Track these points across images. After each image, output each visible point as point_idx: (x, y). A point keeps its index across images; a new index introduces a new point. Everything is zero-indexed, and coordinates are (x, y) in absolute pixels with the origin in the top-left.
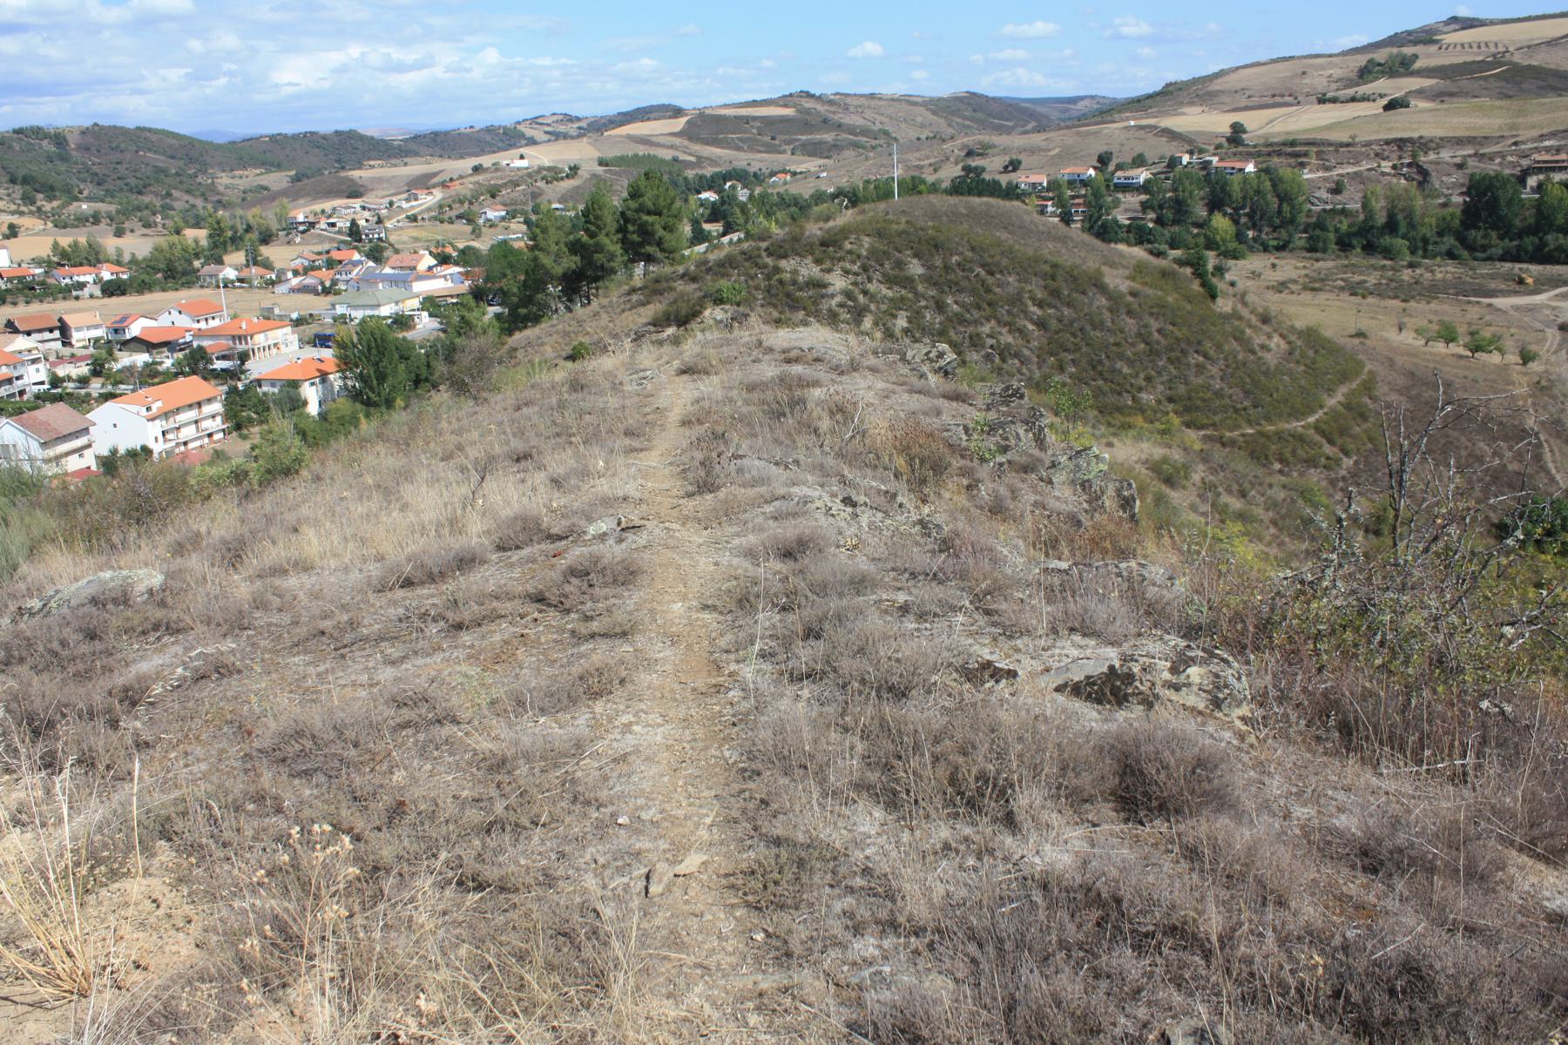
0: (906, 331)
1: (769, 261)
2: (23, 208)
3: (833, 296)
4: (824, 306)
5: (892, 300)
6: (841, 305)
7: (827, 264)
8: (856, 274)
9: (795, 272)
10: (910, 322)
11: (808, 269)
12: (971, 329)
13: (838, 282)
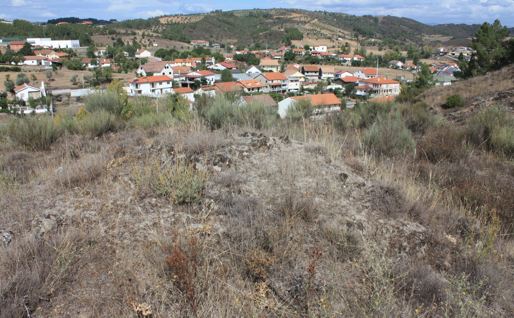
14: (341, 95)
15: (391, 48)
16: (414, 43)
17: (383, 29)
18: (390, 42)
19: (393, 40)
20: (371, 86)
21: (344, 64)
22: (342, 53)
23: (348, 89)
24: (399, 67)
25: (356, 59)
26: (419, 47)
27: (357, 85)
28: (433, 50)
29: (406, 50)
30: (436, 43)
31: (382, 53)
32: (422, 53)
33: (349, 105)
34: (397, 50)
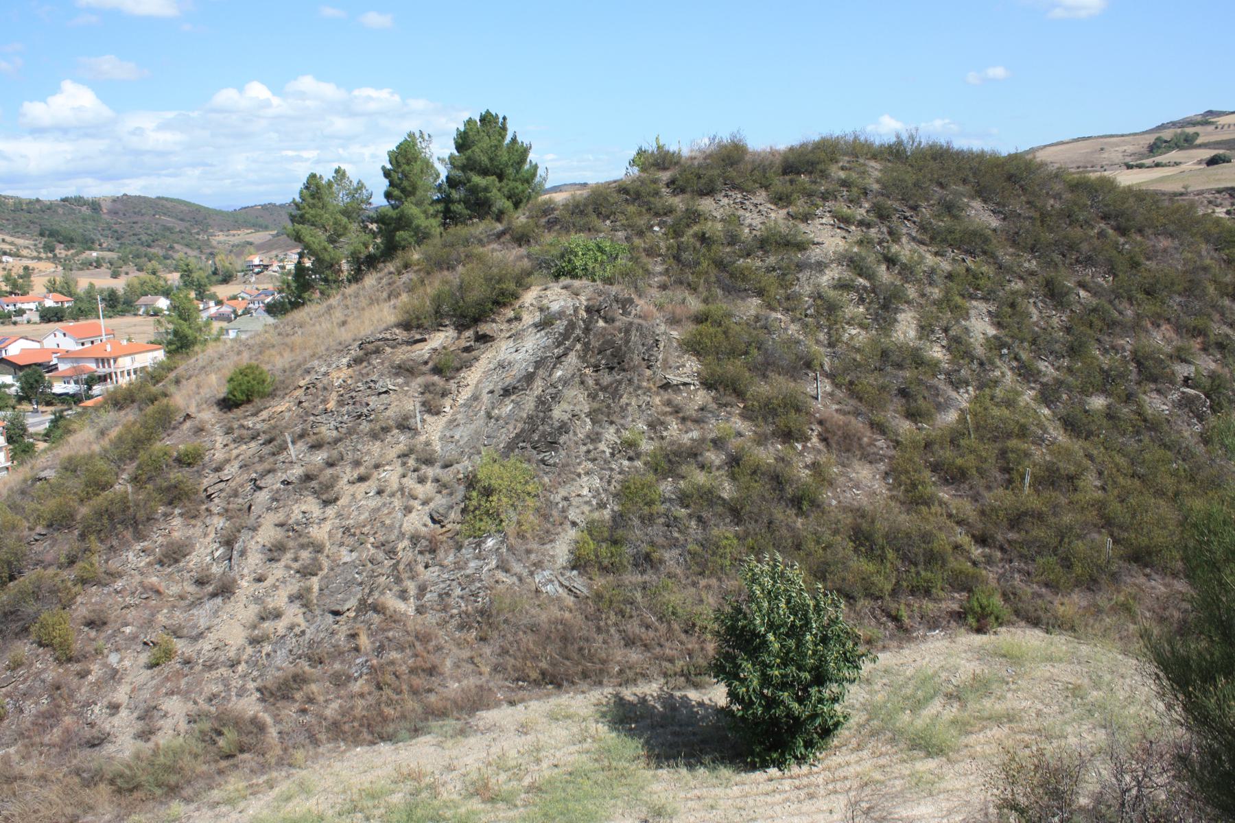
0: (996, 345)
1: (678, 202)
2: (43, 255)
3: (820, 266)
4: (804, 287)
5: (950, 276)
6: (842, 286)
7: (800, 205)
8: (861, 223)
9: (732, 220)
10: (999, 325)
11: (760, 216)
12: (1127, 343)
13: (828, 240)
14: (13, 402)
15: (140, 269)
16: (196, 253)
17: (116, 227)
18: (137, 256)
19: (143, 249)
20: (93, 366)
21: (18, 319)
22: (11, 293)
23: (27, 382)
24: (161, 310)
25: (49, 303)
26: (208, 259)
27: (53, 368)
29: (176, 270)
30: (240, 249)
31: (119, 285)
32: (215, 273)
33: (34, 425)
34: (154, 273)
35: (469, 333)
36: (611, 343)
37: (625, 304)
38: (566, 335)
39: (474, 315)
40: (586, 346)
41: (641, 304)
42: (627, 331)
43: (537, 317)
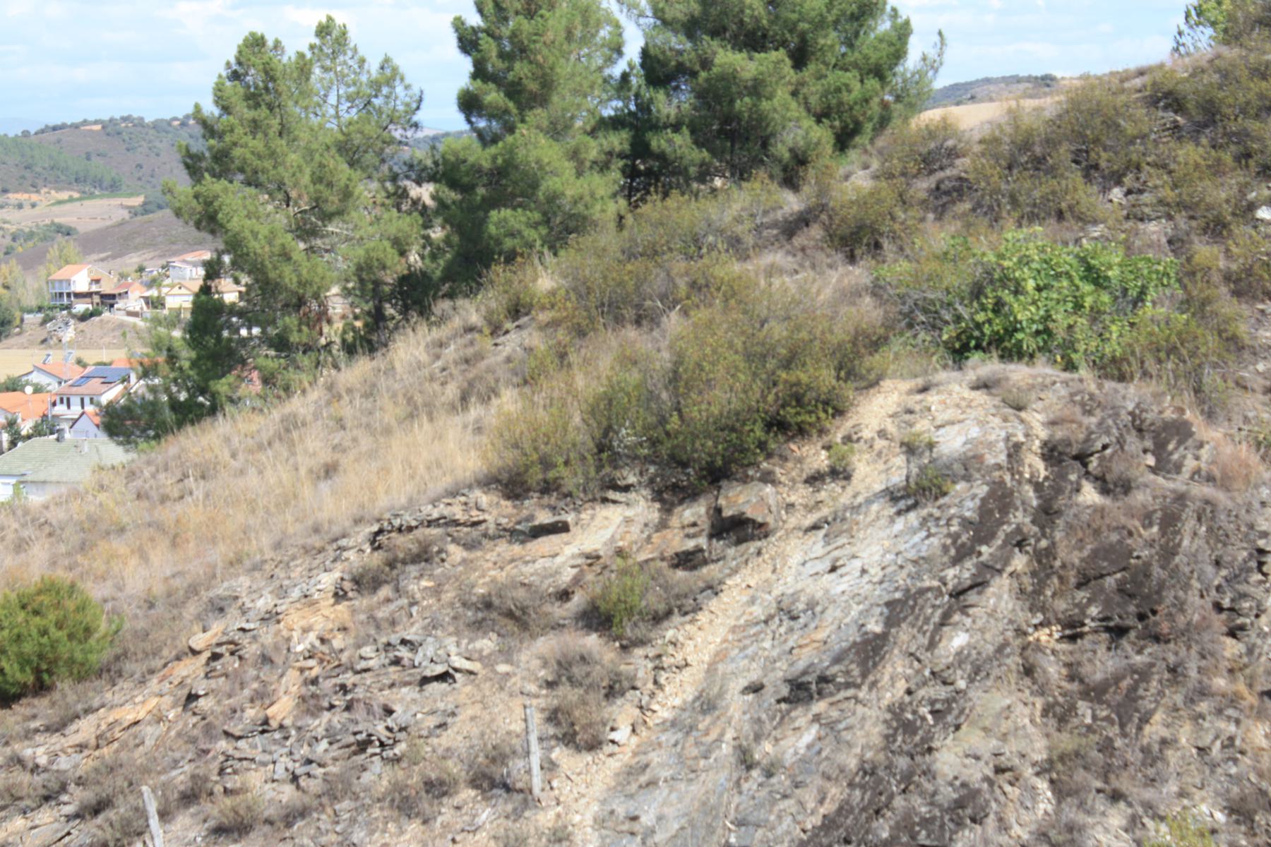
28: (30, 289)
35: (695, 512)
36: (1118, 555)
37: (1165, 438)
38: (982, 528)
39: (710, 458)
40: (1043, 559)
41: (1215, 442)
42: (1170, 521)
43: (898, 471)
